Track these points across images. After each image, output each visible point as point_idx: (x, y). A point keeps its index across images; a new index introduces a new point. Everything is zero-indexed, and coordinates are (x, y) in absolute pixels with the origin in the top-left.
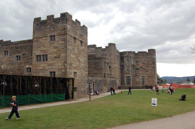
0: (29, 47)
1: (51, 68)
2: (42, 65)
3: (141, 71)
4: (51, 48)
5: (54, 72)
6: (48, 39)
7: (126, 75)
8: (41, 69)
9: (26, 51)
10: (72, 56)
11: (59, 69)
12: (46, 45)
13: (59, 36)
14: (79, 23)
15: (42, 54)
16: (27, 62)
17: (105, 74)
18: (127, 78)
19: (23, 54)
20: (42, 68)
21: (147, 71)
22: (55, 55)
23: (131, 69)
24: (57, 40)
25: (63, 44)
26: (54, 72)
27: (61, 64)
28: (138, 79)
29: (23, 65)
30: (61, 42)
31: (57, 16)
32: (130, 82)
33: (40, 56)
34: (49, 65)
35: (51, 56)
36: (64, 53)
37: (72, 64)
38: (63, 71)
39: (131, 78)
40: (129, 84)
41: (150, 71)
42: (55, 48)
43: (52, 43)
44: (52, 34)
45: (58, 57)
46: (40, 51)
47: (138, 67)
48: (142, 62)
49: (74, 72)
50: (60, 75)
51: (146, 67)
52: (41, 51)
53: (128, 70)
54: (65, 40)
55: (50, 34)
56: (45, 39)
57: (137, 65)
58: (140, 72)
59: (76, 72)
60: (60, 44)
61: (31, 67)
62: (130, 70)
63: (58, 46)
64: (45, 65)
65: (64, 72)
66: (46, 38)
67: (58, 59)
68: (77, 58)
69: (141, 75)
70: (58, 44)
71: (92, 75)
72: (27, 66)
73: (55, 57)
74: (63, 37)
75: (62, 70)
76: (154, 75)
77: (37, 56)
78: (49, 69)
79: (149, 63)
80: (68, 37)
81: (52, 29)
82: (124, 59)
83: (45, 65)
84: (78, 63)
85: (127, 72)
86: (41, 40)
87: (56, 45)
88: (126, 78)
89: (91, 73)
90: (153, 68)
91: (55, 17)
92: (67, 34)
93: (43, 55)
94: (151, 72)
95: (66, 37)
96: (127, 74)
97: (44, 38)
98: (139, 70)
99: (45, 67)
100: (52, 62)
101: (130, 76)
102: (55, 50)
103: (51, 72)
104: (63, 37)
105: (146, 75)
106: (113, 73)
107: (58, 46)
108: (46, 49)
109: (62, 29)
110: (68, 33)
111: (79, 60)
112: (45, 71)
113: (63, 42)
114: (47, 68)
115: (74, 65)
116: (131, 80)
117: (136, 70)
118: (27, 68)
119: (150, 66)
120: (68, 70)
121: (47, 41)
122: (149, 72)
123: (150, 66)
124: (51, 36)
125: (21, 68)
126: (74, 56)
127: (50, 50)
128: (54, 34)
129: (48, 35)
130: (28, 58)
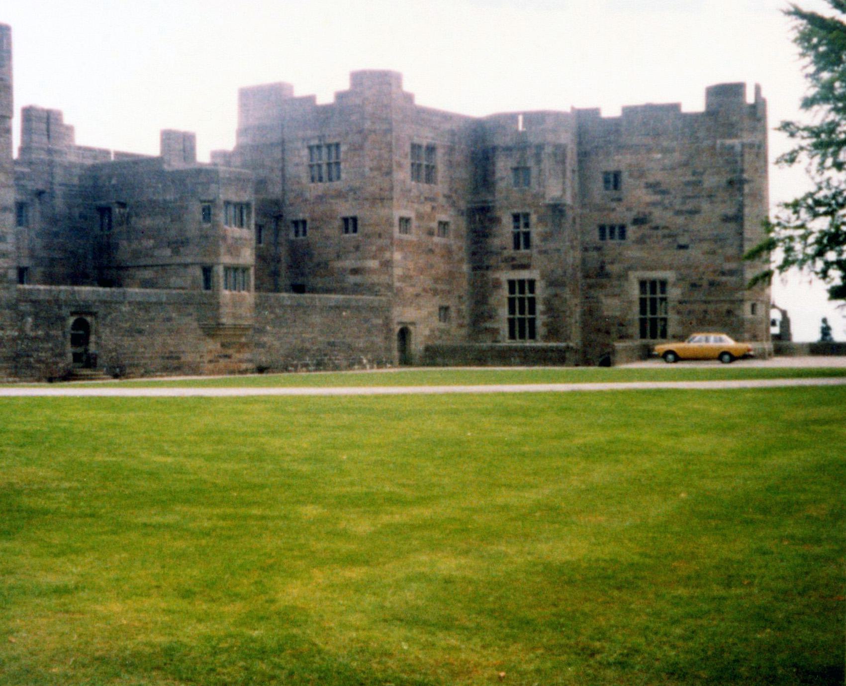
3: (641, 241)
7: (505, 276)
17: (207, 271)
18: (512, 291)
21: (683, 241)
23: (536, 231)
28: (616, 302)
32: (532, 322)
39: (674, 293)
40: (522, 336)
41: (706, 246)
47: (620, 215)
48: (651, 179)
51: (679, 213)
53: (522, 240)
57: (614, 205)
58: (633, 253)
62: (535, 239)
69: (634, 277)
71: (148, 274)
76: (732, 273)
79: (698, 183)
82: (494, 164)
85: (510, 252)
88: (505, 292)
89: (142, 262)
90: (726, 219)
94: (714, 253)
96: (514, 268)
98: (623, 235)
101: (532, 283)
105: (669, 275)
106: (373, 264)
116: (540, 307)
117: (603, 237)
119: (705, 206)
122: (696, 253)
123: (705, 206)
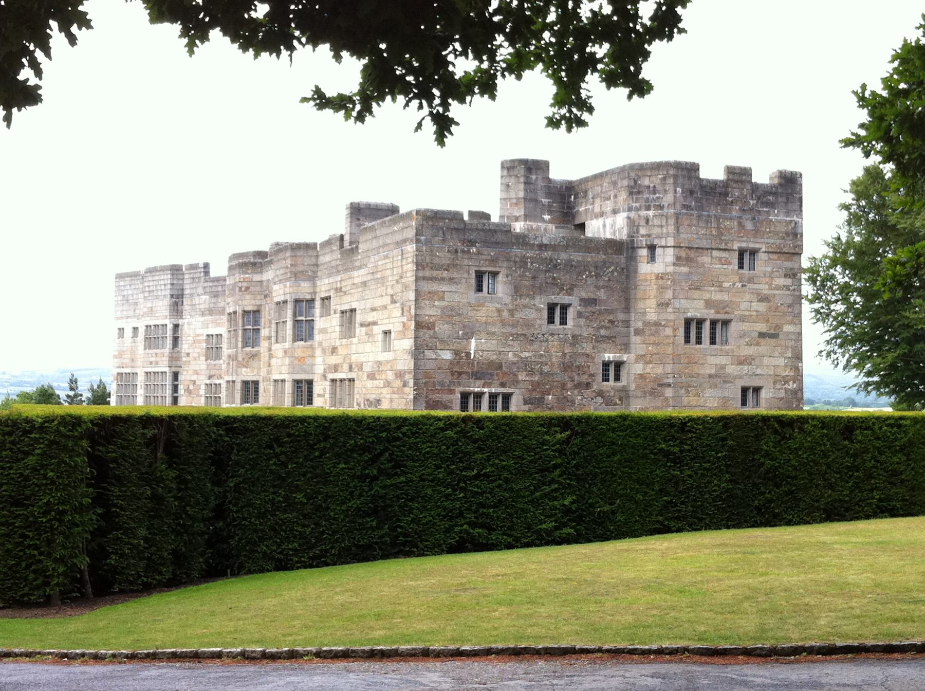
0: (612, 272)
1: (746, 374)
9: (598, 288)
15: (711, 314)
20: (713, 371)
22: (762, 327)
33: (700, 322)
35: (745, 326)
43: (751, 280)
46: (701, 304)
55: (744, 245)
56: (720, 259)
64: (723, 360)
73: (762, 335)
81: (749, 225)
83: (723, 360)
99: (723, 367)
108: (725, 297)
112: (725, 382)
114: (731, 369)
127: (744, 306)
128: (757, 246)
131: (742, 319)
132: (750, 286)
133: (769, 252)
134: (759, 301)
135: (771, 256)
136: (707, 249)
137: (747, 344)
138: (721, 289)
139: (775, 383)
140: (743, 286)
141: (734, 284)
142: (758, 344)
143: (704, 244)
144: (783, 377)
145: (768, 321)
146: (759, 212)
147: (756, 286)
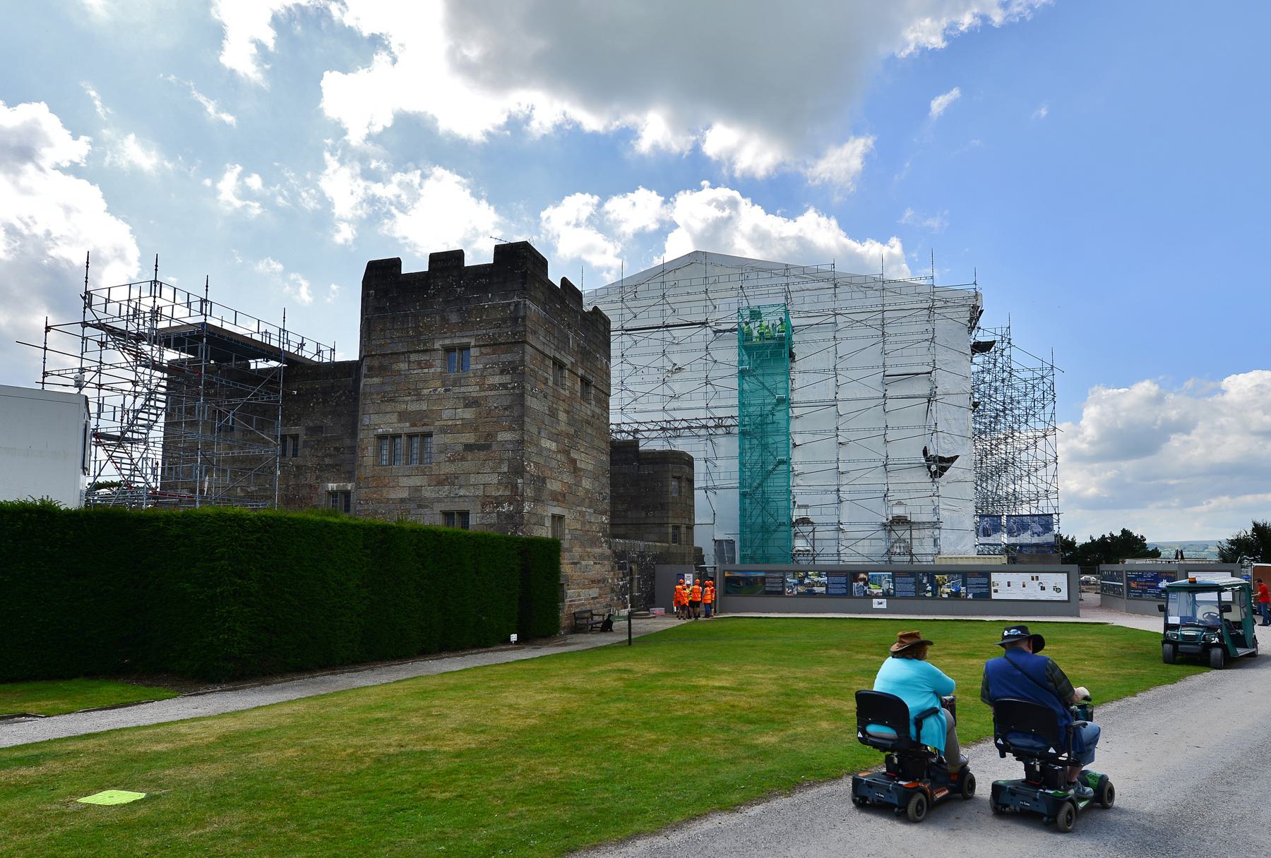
2: (405, 482)
4: (450, 403)
5: (464, 515)
6: (438, 363)
8: (402, 500)
10: (548, 444)
11: (487, 501)
12: (425, 392)
13: (488, 350)
14: (577, 295)
15: (406, 427)
16: (333, 466)
19: (308, 429)
20: (405, 495)
22: (470, 438)
24: (481, 366)
25: (504, 386)
26: (464, 515)
27: (494, 479)
29: (310, 478)
30: (497, 380)
31: (480, 254)
33: (395, 437)
34: (440, 483)
35: (448, 439)
36: (511, 429)
37: (544, 480)
38: (506, 508)
42: (471, 403)
43: (456, 383)
44: (457, 341)
45: (486, 447)
46: (394, 417)
49: (553, 516)
50: (491, 525)
52: (403, 416)
54: (515, 369)
55: (447, 342)
56: (419, 363)
59: (561, 518)
60: (493, 387)
61: (349, 486)
63: (483, 394)
64: (417, 481)
65: (510, 516)
66: (423, 357)
67: (482, 454)
68: (567, 453)
70: (481, 385)
72: (332, 486)
73: (468, 448)
74: (507, 358)
75: (500, 504)
77: (381, 437)
78: (439, 500)
80: (527, 358)
81: (454, 318)
83: (417, 481)
84: (567, 478)
86: (403, 366)
87: (473, 390)
91: (468, 262)
92: (525, 342)
93: (410, 436)
95: (518, 358)
97: (413, 357)
99: (417, 489)
100: (448, 469)
102: (469, 414)
103: (448, 515)
104: (507, 358)
107: (483, 394)
109: (504, 320)
110: (530, 338)
111: (574, 461)
112: (420, 506)
113: (506, 379)
114: (428, 493)
115: (554, 486)
118: (333, 494)
120: (527, 507)
121: (432, 370)
124: (448, 350)
125: (304, 492)
126: (553, 446)
127: (446, 414)
128: (465, 340)
129: (437, 346)
130: (337, 449)
131: (444, 430)
132: (456, 390)
133: (480, 346)
134: (466, 406)
135: (484, 350)
136: (403, 353)
137: (449, 461)
138: (419, 397)
139: (484, 505)
140: (446, 390)
141: (435, 390)
142: (463, 459)
143: (400, 348)
144: (496, 498)
145: (476, 429)
146: (468, 300)
147: (463, 389)
